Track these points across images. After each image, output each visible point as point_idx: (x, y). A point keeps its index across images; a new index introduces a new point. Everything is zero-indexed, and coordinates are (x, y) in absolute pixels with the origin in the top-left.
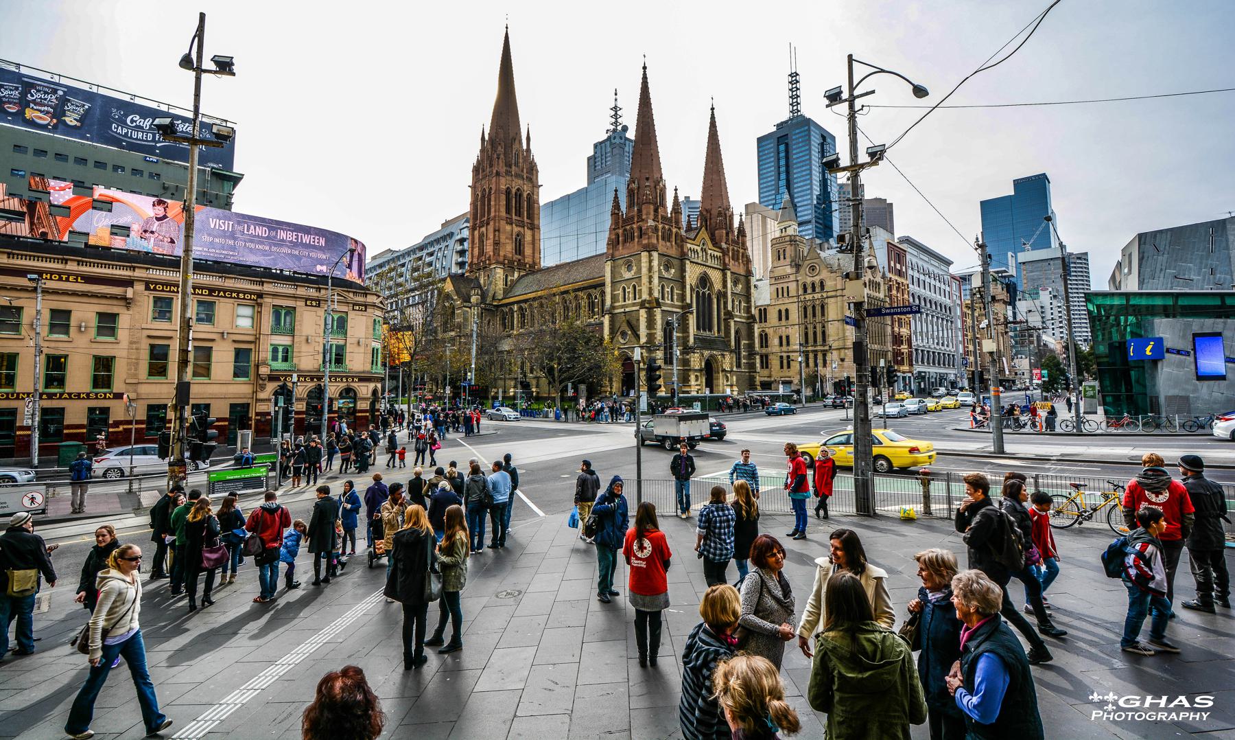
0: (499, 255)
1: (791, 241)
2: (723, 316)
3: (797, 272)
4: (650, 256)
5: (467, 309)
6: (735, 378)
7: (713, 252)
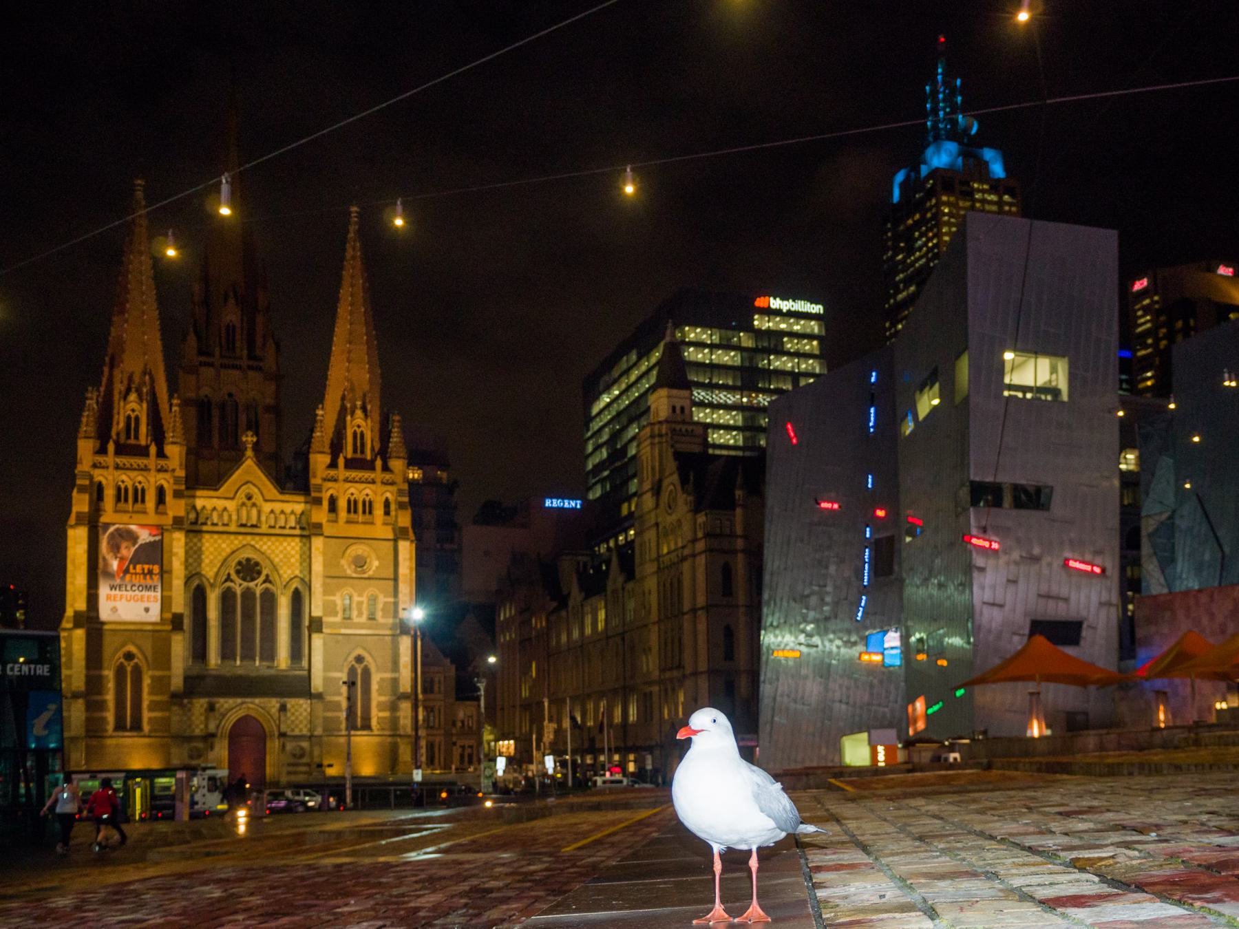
7: (278, 507)
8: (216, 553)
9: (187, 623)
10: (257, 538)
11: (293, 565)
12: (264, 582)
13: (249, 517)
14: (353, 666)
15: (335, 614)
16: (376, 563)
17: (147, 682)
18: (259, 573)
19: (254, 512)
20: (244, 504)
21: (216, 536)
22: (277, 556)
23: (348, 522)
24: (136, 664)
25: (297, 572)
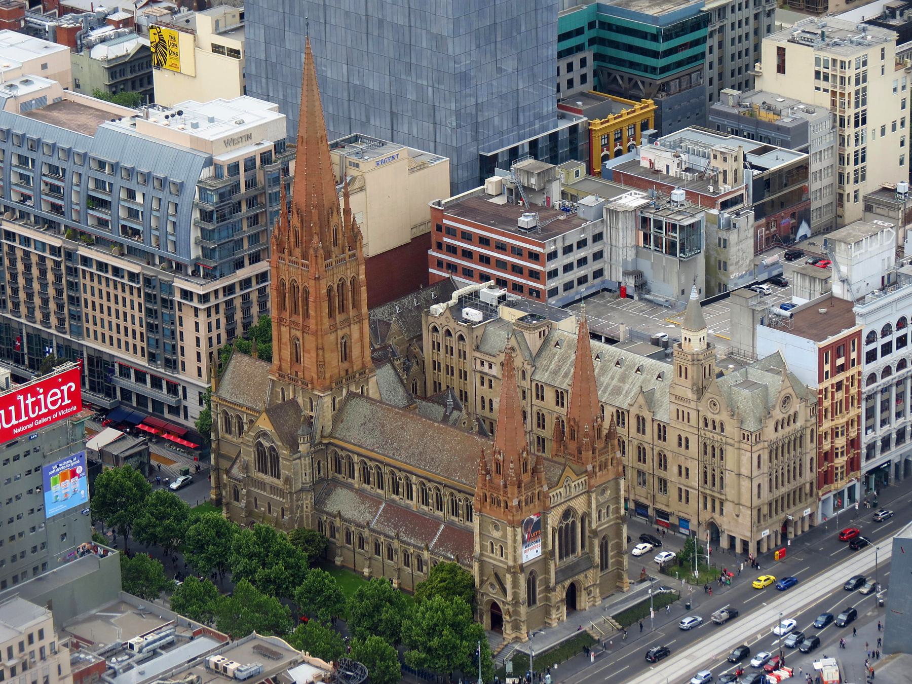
0: (325, 378)
1: (693, 360)
2: (587, 534)
3: (699, 399)
4: (515, 530)
5: (298, 461)
6: (598, 590)
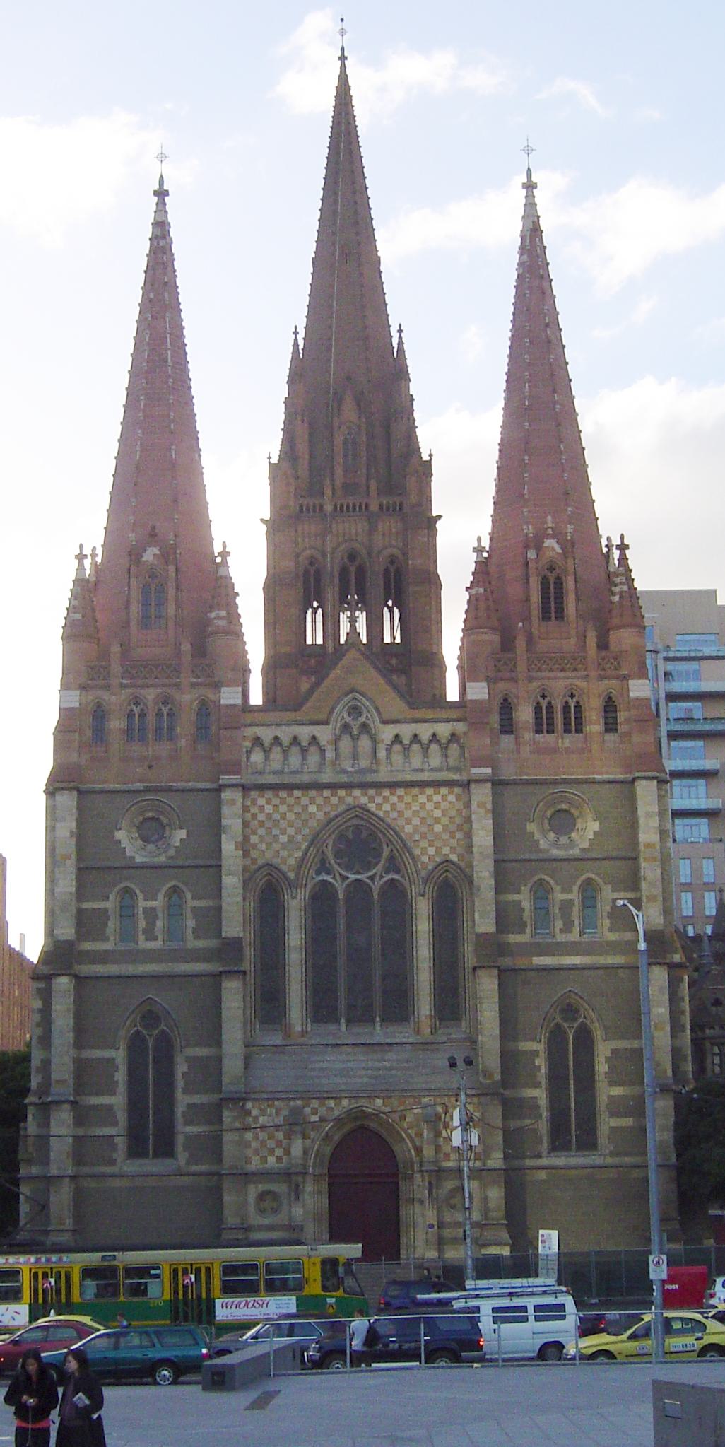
7: (406, 731)
8: (298, 823)
9: (249, 952)
10: (371, 792)
11: (437, 835)
12: (387, 872)
13: (355, 756)
14: (558, 1026)
15: (521, 928)
16: (596, 826)
17: (181, 1068)
18: (379, 855)
19: (365, 742)
20: (346, 727)
21: (297, 793)
22: (408, 822)
23: (539, 751)
24: (163, 1031)
25: (446, 850)
